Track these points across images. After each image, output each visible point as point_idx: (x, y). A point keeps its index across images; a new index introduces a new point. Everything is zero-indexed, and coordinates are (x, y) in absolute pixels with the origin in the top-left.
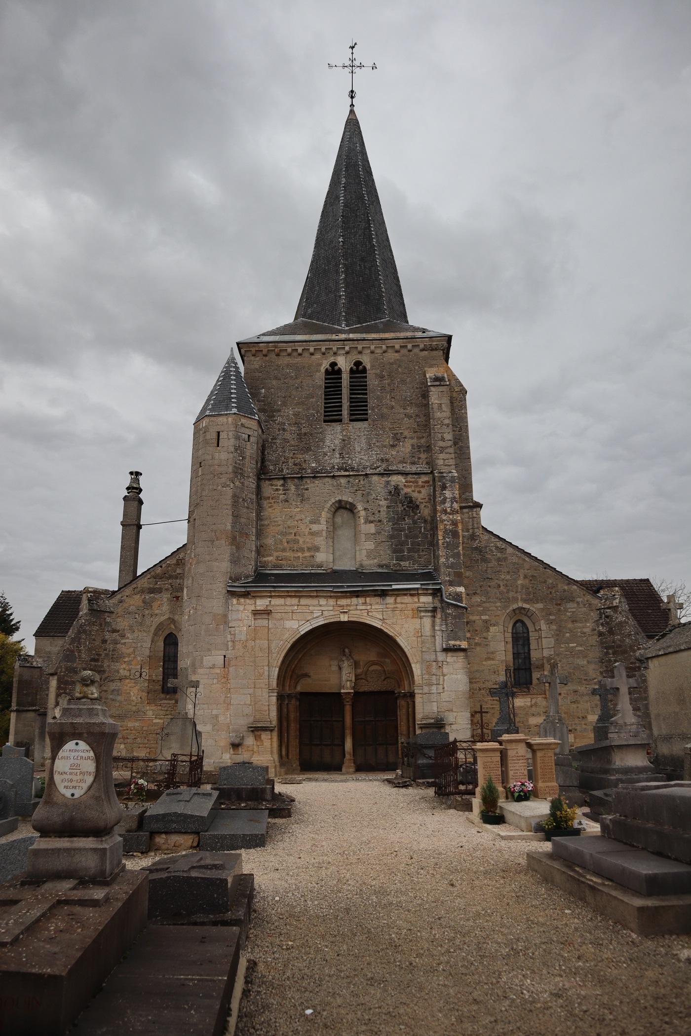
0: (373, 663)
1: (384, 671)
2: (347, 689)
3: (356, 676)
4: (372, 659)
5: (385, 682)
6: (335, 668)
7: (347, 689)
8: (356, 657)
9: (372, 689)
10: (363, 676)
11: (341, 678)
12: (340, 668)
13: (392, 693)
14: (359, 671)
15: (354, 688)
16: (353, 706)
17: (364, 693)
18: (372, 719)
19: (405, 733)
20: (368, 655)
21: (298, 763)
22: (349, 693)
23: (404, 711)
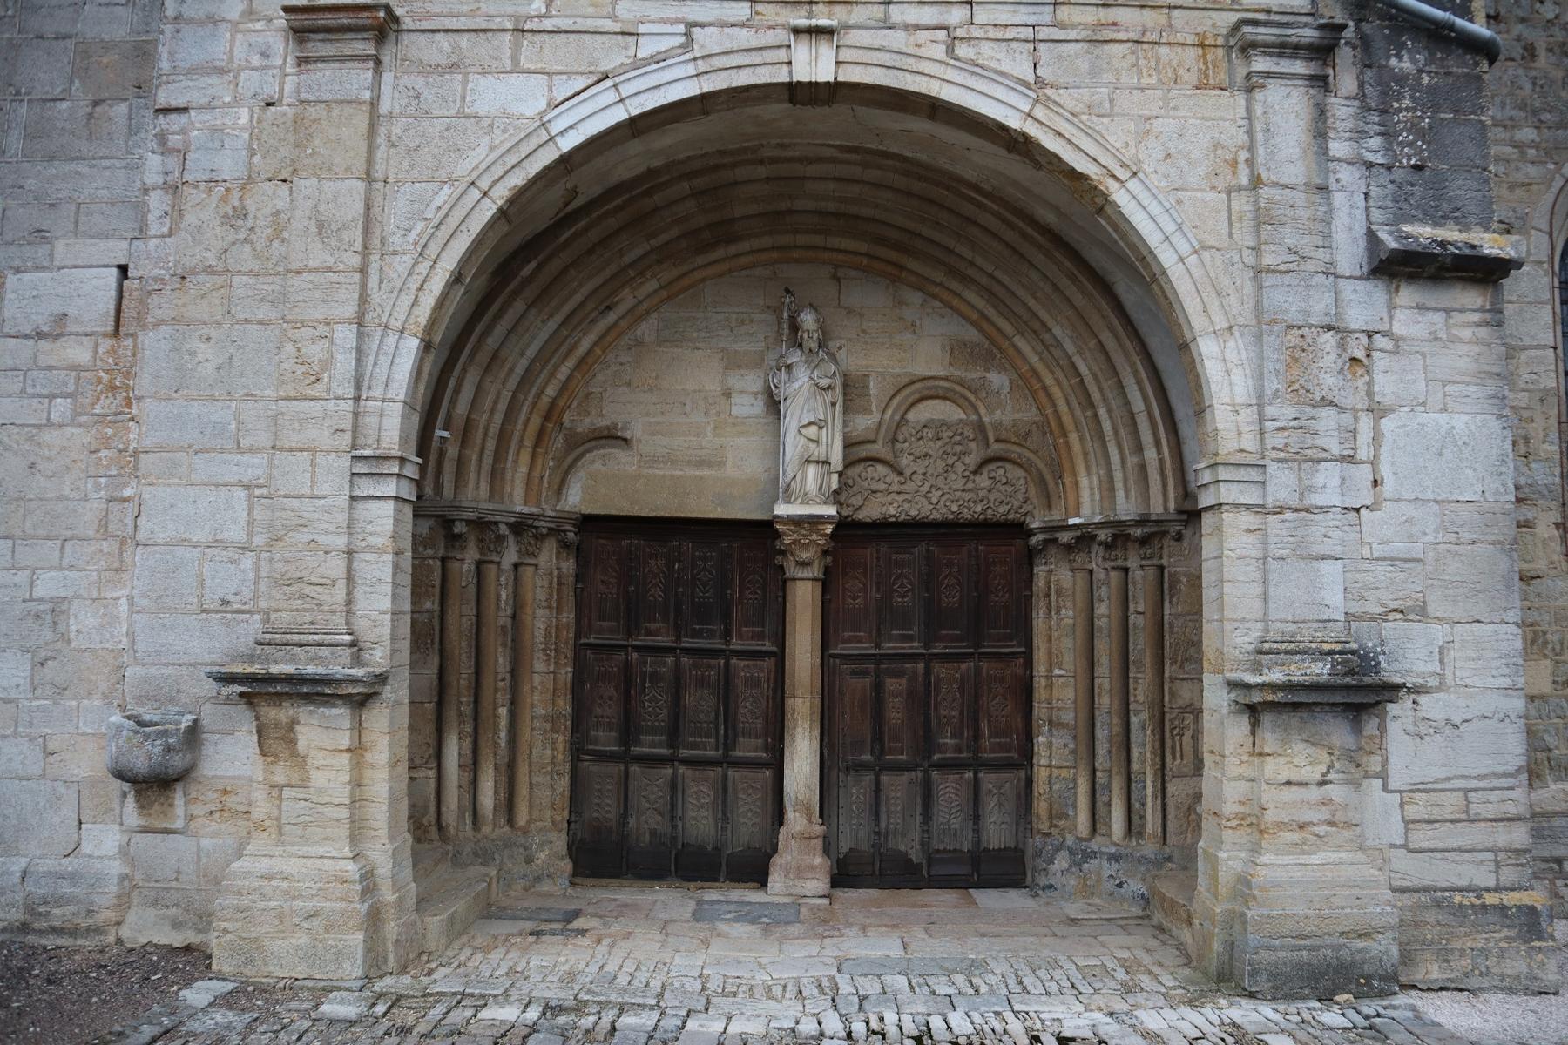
0: (929, 390)
1: (980, 427)
2: (807, 499)
3: (848, 446)
4: (921, 369)
5: (983, 481)
6: (748, 406)
7: (807, 499)
8: (853, 359)
9: (919, 509)
10: (878, 449)
11: (775, 450)
12: (774, 405)
13: (1016, 529)
14: (863, 423)
15: (836, 497)
16: (827, 583)
17: (884, 530)
18: (915, 647)
19: (1068, 717)
20: (906, 346)
21: (560, 842)
22: (814, 521)
23: (1069, 614)
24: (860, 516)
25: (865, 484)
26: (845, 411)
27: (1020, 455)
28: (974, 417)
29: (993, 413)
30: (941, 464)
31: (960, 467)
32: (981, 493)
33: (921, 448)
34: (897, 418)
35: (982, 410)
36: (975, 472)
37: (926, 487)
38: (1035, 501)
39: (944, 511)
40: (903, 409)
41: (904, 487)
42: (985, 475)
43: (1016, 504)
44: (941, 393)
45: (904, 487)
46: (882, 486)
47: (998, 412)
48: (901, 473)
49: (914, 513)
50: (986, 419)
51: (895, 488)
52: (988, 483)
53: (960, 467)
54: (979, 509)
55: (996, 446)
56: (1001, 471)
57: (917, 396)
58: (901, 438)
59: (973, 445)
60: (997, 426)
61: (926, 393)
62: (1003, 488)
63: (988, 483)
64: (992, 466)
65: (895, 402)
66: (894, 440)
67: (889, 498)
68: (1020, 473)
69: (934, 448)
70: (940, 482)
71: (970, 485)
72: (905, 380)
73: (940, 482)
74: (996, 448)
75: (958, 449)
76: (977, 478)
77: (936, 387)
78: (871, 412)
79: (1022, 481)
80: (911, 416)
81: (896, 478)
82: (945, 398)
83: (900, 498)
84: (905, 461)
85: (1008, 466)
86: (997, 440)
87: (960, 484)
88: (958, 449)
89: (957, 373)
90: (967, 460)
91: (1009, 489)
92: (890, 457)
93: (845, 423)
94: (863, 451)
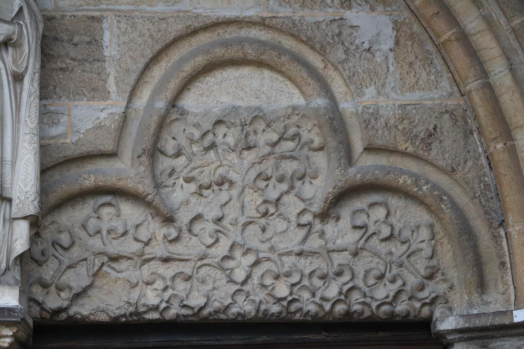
1: (335, 122)
5: (341, 232)
10: (124, 170)
24: (84, 309)
25: (96, 243)
26: (45, 92)
27: (417, 179)
28: (320, 102)
29: (359, 93)
30: (253, 201)
31: (292, 205)
32: (338, 259)
33: (210, 167)
34: (161, 104)
35: (338, 87)
36: (324, 216)
37: (222, 249)
38: (453, 274)
39: (261, 295)
40: (173, 85)
41: (177, 249)
42: (345, 222)
43: (412, 281)
44: (251, 52)
45: (177, 249)
46: (130, 247)
47: (370, 91)
48: (169, 220)
49: (196, 300)
50: (347, 106)
51: (158, 249)
52: (351, 238)
53: (292, 205)
54: (332, 291)
55: (368, 161)
56: (380, 213)
57: (201, 60)
58: (170, 147)
59: (320, 160)
60: (369, 118)
61: (219, 52)
62: (383, 248)
63: (351, 238)
64: (360, 203)
65: (157, 73)
66: (154, 152)
67: (146, 271)
68: (418, 215)
69: (239, 167)
70: (253, 237)
71: (315, 243)
72: (176, 28)
73: (253, 237)
74: (367, 165)
75: (289, 167)
76: (330, 228)
77: (241, 42)
78: (105, 95)
79: (425, 233)
80: (190, 101)
81: (154, 228)
82: (260, 64)
83: (169, 271)
84: (179, 194)
85: (394, 201)
86: (369, 149)
87: (293, 239)
88: (289, 167)
89: (284, 12)
90: (308, 190)
91: (398, 249)
92: (144, 187)
93: (45, 116)
94: (89, 176)
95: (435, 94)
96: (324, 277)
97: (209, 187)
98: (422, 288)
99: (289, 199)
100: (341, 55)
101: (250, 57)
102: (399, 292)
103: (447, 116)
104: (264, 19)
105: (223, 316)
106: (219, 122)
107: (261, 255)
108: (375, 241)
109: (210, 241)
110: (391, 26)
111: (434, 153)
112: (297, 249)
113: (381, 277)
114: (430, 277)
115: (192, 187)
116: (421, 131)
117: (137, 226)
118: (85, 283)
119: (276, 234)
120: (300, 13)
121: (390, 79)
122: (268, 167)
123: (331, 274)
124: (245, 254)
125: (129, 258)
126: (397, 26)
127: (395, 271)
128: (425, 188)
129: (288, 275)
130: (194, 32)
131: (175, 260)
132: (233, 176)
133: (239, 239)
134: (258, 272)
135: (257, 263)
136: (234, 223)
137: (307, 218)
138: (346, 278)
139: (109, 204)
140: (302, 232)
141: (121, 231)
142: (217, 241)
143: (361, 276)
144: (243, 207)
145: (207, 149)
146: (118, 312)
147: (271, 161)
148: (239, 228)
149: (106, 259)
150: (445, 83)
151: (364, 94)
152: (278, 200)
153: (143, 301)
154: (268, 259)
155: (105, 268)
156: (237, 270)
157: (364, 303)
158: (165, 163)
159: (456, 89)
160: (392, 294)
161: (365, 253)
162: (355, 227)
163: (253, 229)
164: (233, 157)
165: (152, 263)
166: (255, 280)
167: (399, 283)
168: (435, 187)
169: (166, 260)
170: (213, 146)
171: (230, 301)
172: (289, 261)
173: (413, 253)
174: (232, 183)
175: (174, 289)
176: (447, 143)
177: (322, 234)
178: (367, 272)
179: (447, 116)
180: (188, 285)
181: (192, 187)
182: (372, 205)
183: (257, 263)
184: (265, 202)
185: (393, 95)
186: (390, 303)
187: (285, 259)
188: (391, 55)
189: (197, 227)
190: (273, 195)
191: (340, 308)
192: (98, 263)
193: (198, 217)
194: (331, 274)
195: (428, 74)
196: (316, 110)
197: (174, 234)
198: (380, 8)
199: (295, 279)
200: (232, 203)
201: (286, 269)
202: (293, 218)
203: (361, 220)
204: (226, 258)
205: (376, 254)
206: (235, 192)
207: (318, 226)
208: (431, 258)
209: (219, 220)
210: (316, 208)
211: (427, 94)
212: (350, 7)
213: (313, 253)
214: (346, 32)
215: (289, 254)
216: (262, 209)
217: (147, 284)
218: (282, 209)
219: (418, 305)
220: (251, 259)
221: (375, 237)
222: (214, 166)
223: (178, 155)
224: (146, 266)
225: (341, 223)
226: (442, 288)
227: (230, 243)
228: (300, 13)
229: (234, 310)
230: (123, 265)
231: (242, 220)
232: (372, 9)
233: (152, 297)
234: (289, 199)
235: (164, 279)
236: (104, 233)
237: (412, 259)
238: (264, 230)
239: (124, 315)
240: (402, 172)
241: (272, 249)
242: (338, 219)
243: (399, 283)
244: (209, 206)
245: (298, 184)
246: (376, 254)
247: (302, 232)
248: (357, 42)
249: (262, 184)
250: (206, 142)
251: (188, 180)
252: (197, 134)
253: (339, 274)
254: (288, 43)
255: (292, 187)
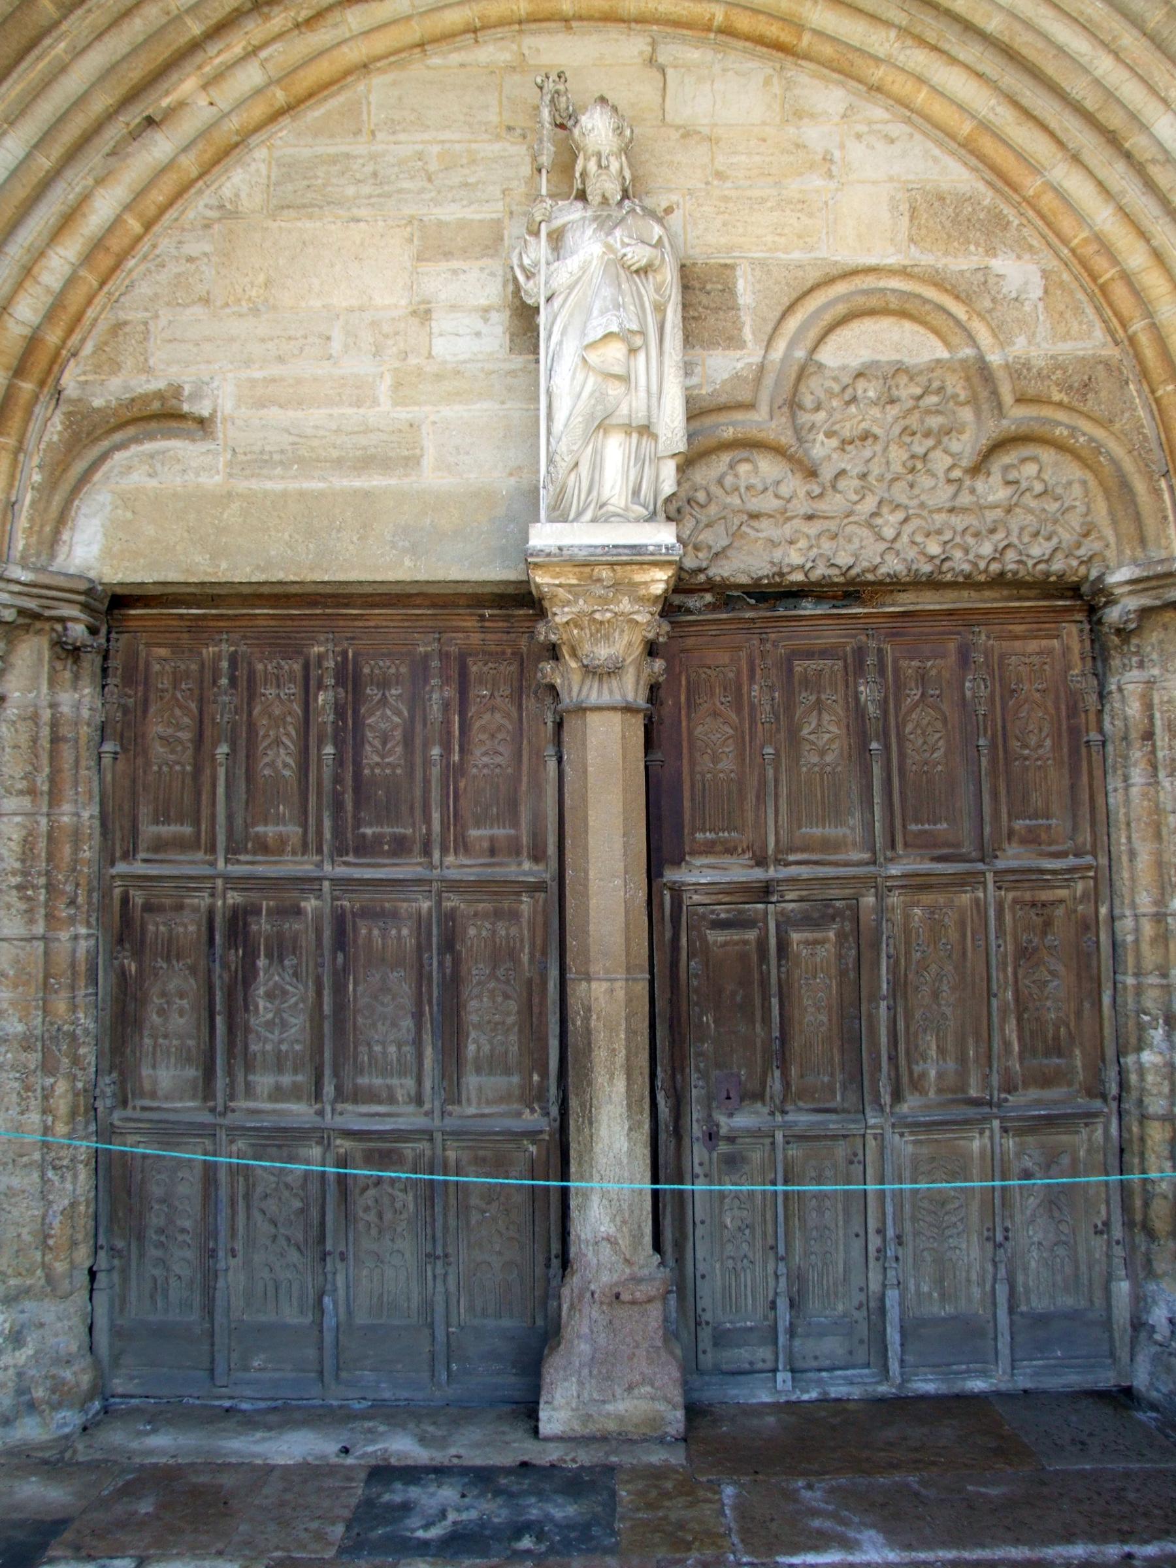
10: (760, 421)
24: (723, 571)
30: (898, 455)
31: (940, 461)
33: (853, 421)
37: (870, 504)
41: (822, 506)
42: (996, 478)
44: (894, 303)
46: (768, 503)
47: (1020, 342)
51: (802, 506)
53: (940, 461)
54: (987, 549)
55: (1021, 412)
57: (841, 309)
58: (808, 401)
60: (1018, 370)
65: (793, 323)
66: (794, 405)
67: (787, 530)
68: (1074, 471)
71: (965, 499)
73: (899, 493)
74: (1018, 415)
76: (980, 485)
80: (828, 355)
81: (793, 484)
82: (903, 314)
83: (813, 529)
84: (821, 448)
85: (1047, 455)
87: (944, 494)
95: (1089, 344)
96: (976, 535)
97: (851, 443)
98: (1079, 545)
99: (937, 454)
100: (987, 304)
101: (892, 306)
102: (1056, 550)
103: (1100, 367)
104: (905, 267)
105: (870, 577)
106: (860, 375)
107: (911, 512)
108: (1028, 499)
109: (855, 498)
110: (1039, 274)
111: (1090, 403)
112: (948, 505)
113: (1036, 534)
114: (1086, 535)
115: (834, 442)
116: (1076, 381)
117: (778, 483)
118: (725, 543)
119: (923, 491)
120: (944, 261)
121: (1040, 329)
122: (913, 421)
123: (984, 532)
124: (892, 511)
125: (771, 516)
126: (1045, 275)
127: (1050, 527)
128: (1081, 439)
129: (939, 532)
130: (830, 280)
131: (819, 517)
132: (876, 430)
133: (886, 495)
134: (908, 529)
135: (906, 520)
136: (880, 478)
137: (957, 474)
138: (1000, 535)
139: (747, 460)
140: (951, 490)
141: (760, 487)
142: (863, 497)
143: (1015, 533)
144: (888, 463)
145: (848, 403)
146: (760, 573)
147: (916, 415)
148: (885, 485)
149: (745, 517)
150: (1099, 333)
151: (1014, 344)
152: (926, 455)
153: (787, 561)
154: (918, 516)
155: (744, 528)
156: (885, 529)
157: (1020, 562)
158: (804, 418)
159: (1109, 339)
160: (1048, 552)
161: (1018, 510)
162: (1008, 483)
163: (901, 485)
164: (875, 412)
165: (795, 521)
166: (905, 538)
167: (1055, 540)
168: (1092, 439)
169: (810, 518)
170: (854, 400)
171: (878, 560)
172: (939, 518)
173: (1068, 509)
174: (876, 437)
175: (819, 547)
176: (1103, 394)
177: (973, 491)
178: (1022, 529)
179: (1100, 367)
180: (834, 544)
181: (834, 442)
182: (1024, 460)
183: (906, 520)
184: (913, 457)
185: (1044, 345)
186: (1047, 561)
187: (936, 516)
188: (1041, 305)
189: (842, 484)
190: (919, 450)
191: (995, 567)
192: (737, 522)
193: (843, 472)
194: (984, 532)
195: (1081, 323)
196: (963, 361)
197: (817, 490)
198: (1027, 256)
199: (947, 537)
200: (876, 459)
201: (938, 525)
202: (941, 475)
203: (1013, 475)
204: (874, 515)
205: (1030, 511)
206: (878, 448)
207: (968, 482)
208: (1087, 515)
209: (863, 476)
210: (965, 463)
211: (1080, 344)
212: (995, 256)
213: (965, 510)
214: (992, 280)
215: (939, 510)
216: (909, 464)
217: (791, 543)
218: (929, 465)
219: (1075, 563)
220: (900, 515)
221: (1028, 494)
222: (855, 421)
223: (818, 408)
224: (788, 526)
225: (991, 479)
226: (1097, 546)
227: (877, 499)
228: (944, 261)
229: (883, 570)
230: (764, 523)
231: (889, 476)
232: (1019, 257)
233: (795, 557)
234: (937, 454)
235: (808, 537)
236: (743, 490)
237: (1066, 516)
238: (912, 486)
239: (767, 576)
240: (1059, 424)
241: (922, 505)
242: (989, 474)
243: (1055, 540)
244: (852, 462)
245: (945, 439)
246: (1030, 511)
247: (951, 490)
248: (1004, 290)
249: (908, 439)
250: (847, 397)
251: (829, 434)
252: (837, 388)
253: (993, 531)
254: (930, 293)
255: (939, 442)
